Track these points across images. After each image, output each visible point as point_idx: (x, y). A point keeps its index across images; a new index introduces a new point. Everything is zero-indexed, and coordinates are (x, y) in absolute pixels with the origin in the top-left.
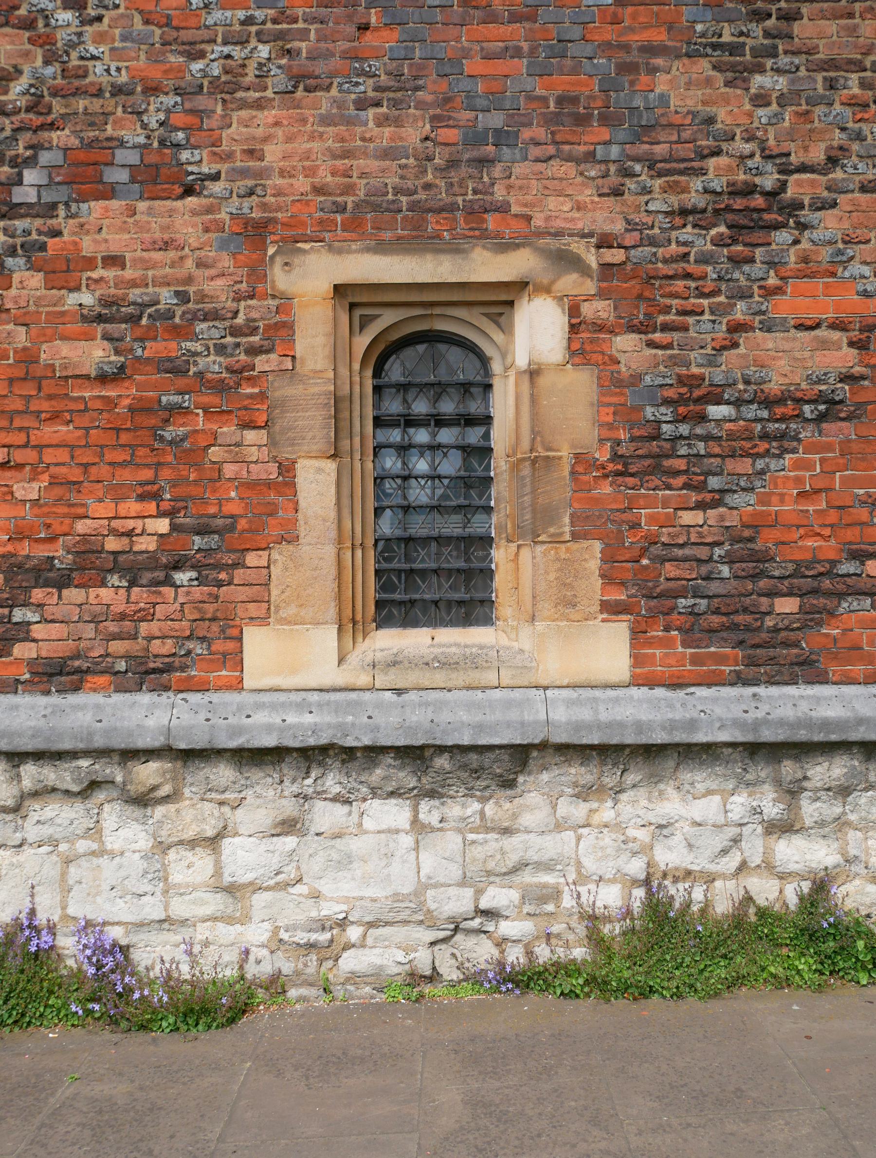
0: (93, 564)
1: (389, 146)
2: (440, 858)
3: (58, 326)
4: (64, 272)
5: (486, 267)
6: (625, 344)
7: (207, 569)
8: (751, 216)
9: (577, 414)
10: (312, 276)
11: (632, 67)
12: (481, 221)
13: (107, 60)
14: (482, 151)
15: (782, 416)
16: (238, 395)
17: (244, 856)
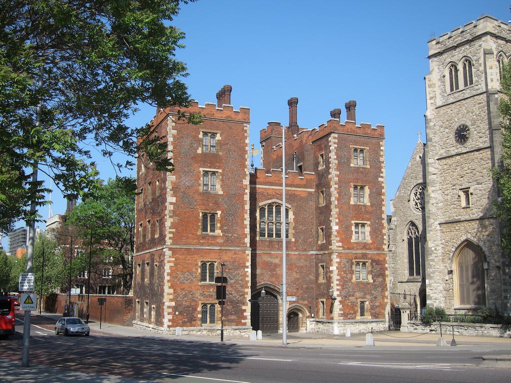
0: (350, 314)
1: (362, 294)
2: (365, 327)
3: (348, 303)
4: (349, 300)
5: (365, 300)
6: (371, 304)
7: (355, 314)
8: (376, 298)
9: (369, 307)
10: (359, 300)
11: (371, 291)
12: (365, 298)
13: (351, 291)
14: (365, 294)
15: (377, 307)
16: (356, 306)
17: (357, 327)
